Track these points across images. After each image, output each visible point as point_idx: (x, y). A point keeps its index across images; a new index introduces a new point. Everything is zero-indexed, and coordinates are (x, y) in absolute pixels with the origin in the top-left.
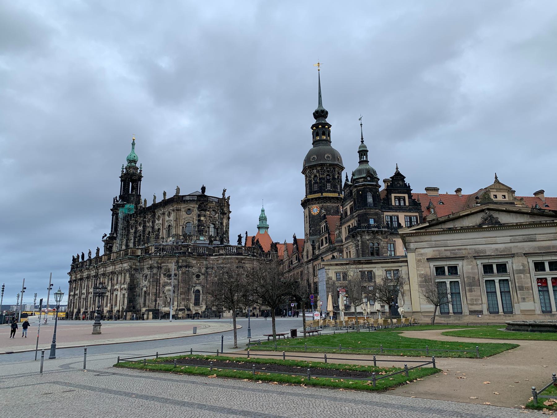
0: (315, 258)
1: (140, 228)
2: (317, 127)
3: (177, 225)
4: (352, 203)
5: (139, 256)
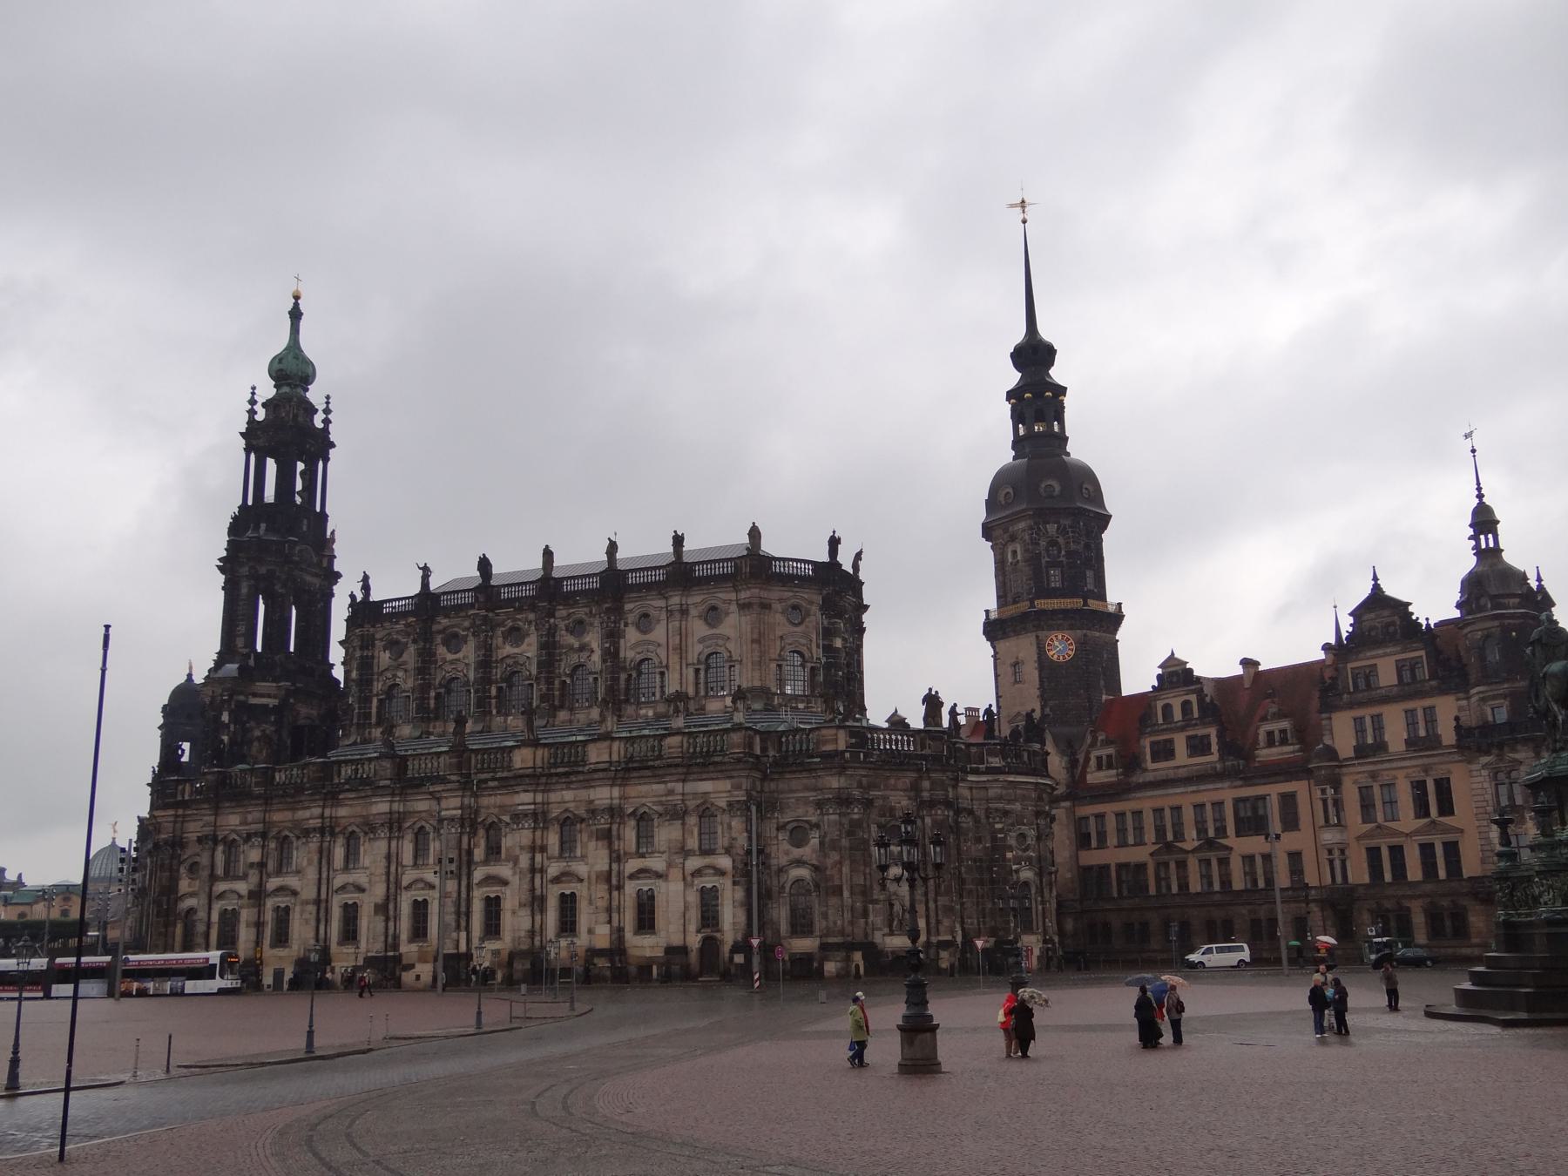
0: (1078, 791)
1: (529, 648)
2: (1038, 395)
3: (762, 654)
4: (1423, 653)
5: (757, 757)
